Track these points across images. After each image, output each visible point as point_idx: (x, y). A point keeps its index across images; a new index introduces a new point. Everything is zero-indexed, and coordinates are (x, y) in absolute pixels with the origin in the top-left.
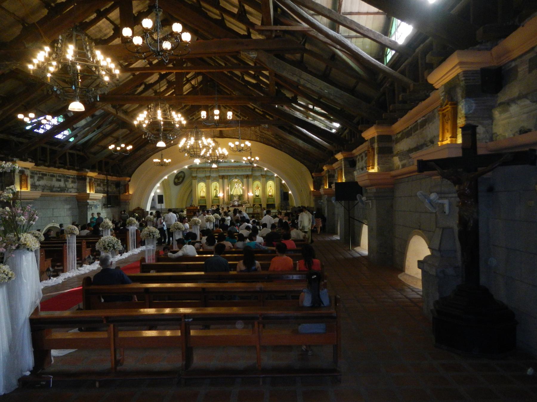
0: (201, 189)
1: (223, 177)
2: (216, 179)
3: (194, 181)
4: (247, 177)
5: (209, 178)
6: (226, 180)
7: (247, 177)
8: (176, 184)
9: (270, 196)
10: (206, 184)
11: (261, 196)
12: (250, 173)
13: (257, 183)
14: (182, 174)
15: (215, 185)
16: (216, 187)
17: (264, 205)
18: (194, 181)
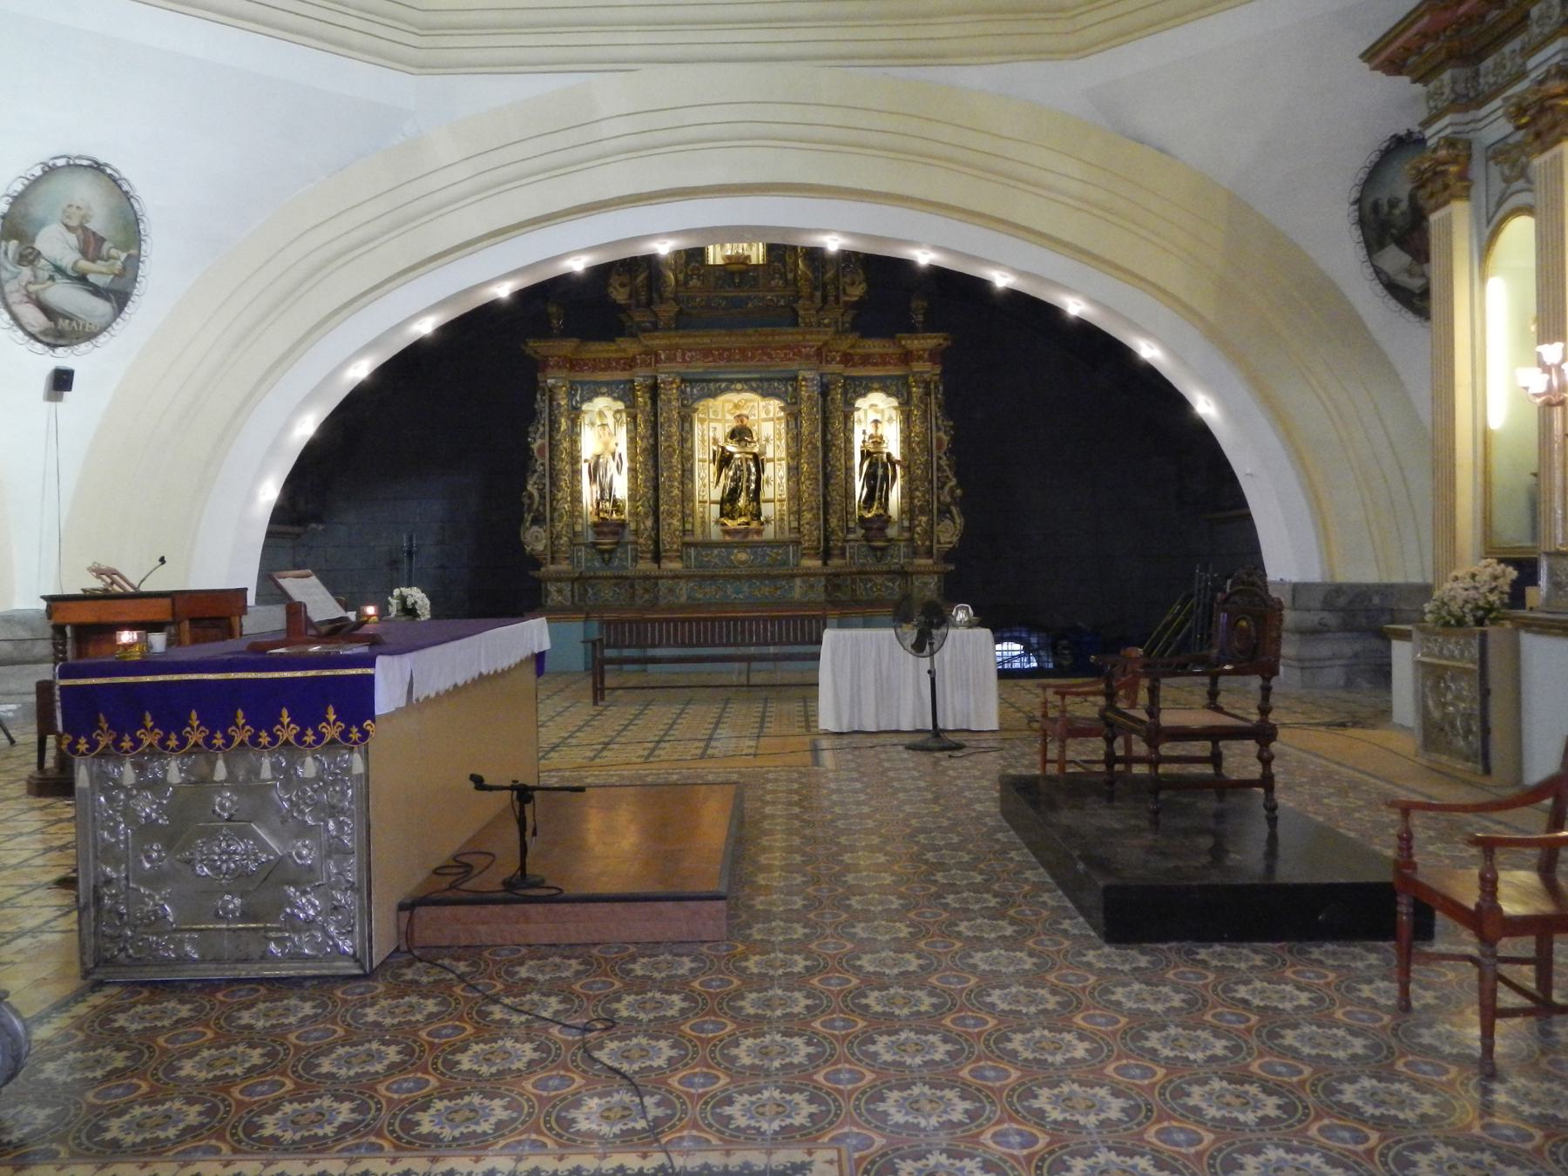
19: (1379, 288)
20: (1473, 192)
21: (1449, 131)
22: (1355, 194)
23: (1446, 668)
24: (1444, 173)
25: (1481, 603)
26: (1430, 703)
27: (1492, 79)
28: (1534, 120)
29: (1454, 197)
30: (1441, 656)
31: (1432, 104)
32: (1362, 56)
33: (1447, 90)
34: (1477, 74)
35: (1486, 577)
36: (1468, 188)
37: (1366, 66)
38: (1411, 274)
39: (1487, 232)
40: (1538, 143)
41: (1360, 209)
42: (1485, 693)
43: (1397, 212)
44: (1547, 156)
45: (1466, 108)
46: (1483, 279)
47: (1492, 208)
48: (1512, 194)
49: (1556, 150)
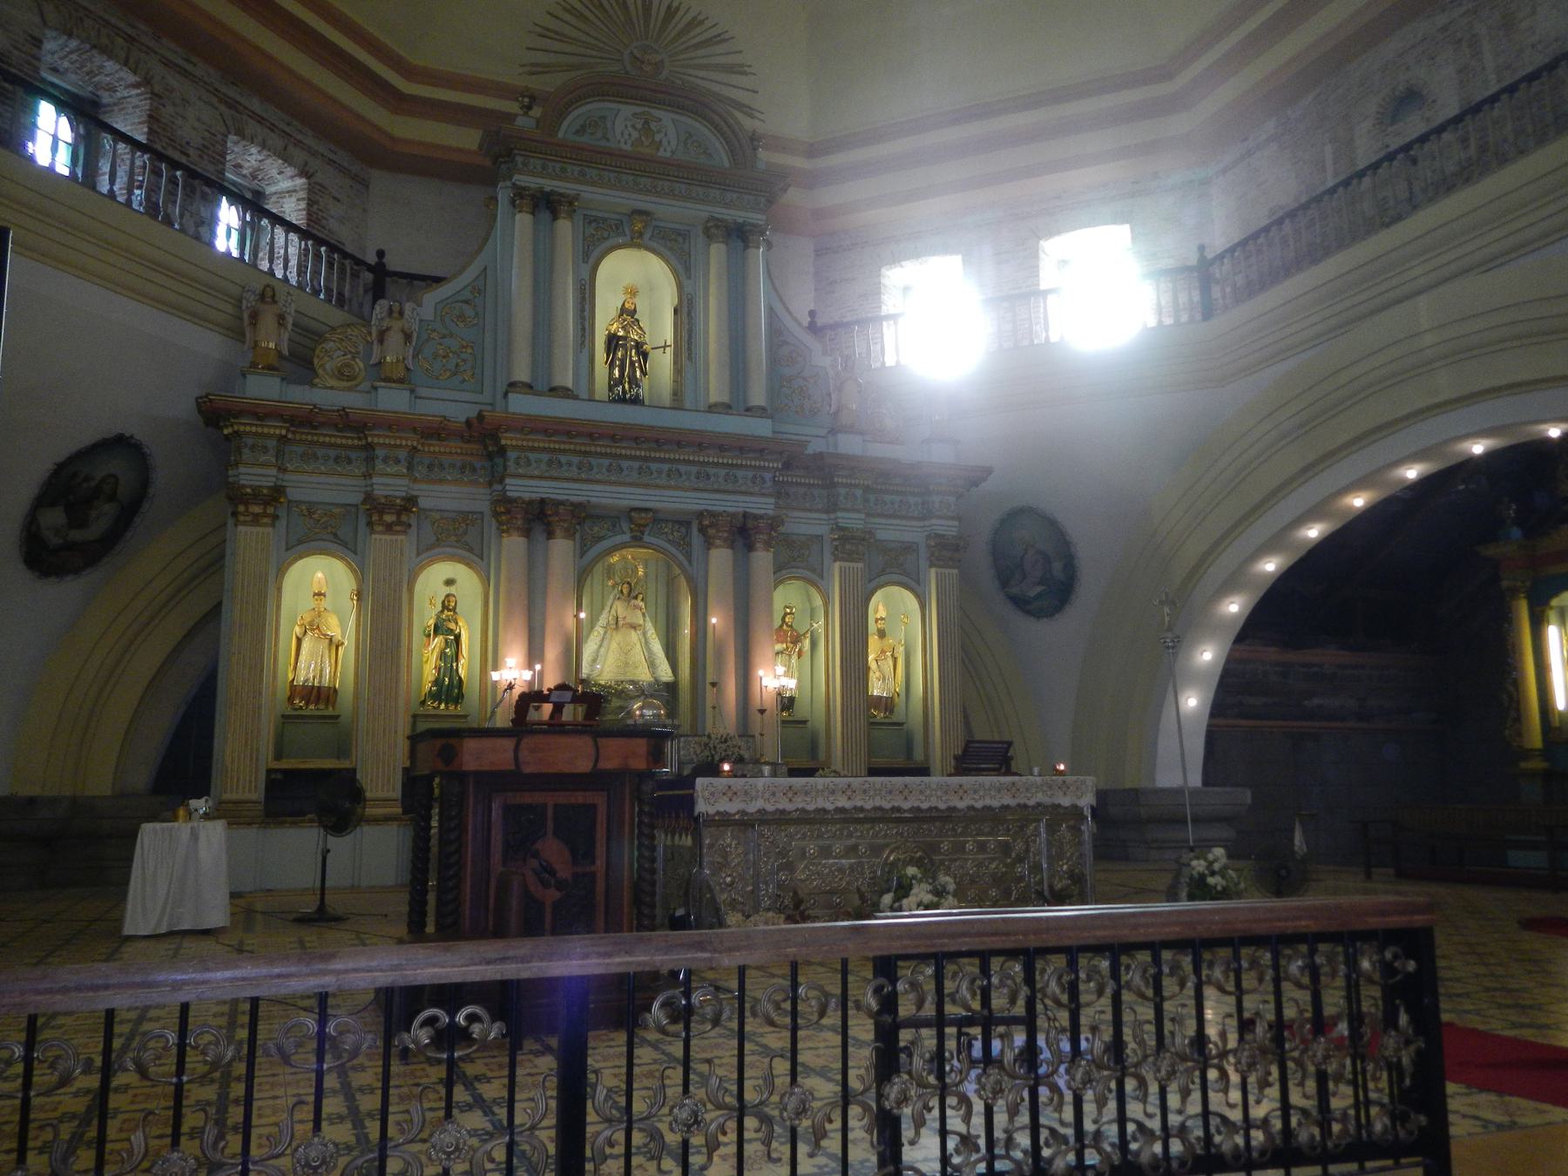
0: (314, 618)
1: (538, 519)
2: (461, 538)
3: (249, 540)
4: (743, 533)
5: (394, 514)
6: (561, 550)
7: (743, 533)
8: (43, 556)
10: (360, 573)
11: (813, 709)
12: (762, 505)
13: (788, 597)
14: (116, 466)
15: (442, 581)
16: (448, 605)
18: (249, 540)
20: (277, 523)
44: (388, 537)
49: (400, 538)
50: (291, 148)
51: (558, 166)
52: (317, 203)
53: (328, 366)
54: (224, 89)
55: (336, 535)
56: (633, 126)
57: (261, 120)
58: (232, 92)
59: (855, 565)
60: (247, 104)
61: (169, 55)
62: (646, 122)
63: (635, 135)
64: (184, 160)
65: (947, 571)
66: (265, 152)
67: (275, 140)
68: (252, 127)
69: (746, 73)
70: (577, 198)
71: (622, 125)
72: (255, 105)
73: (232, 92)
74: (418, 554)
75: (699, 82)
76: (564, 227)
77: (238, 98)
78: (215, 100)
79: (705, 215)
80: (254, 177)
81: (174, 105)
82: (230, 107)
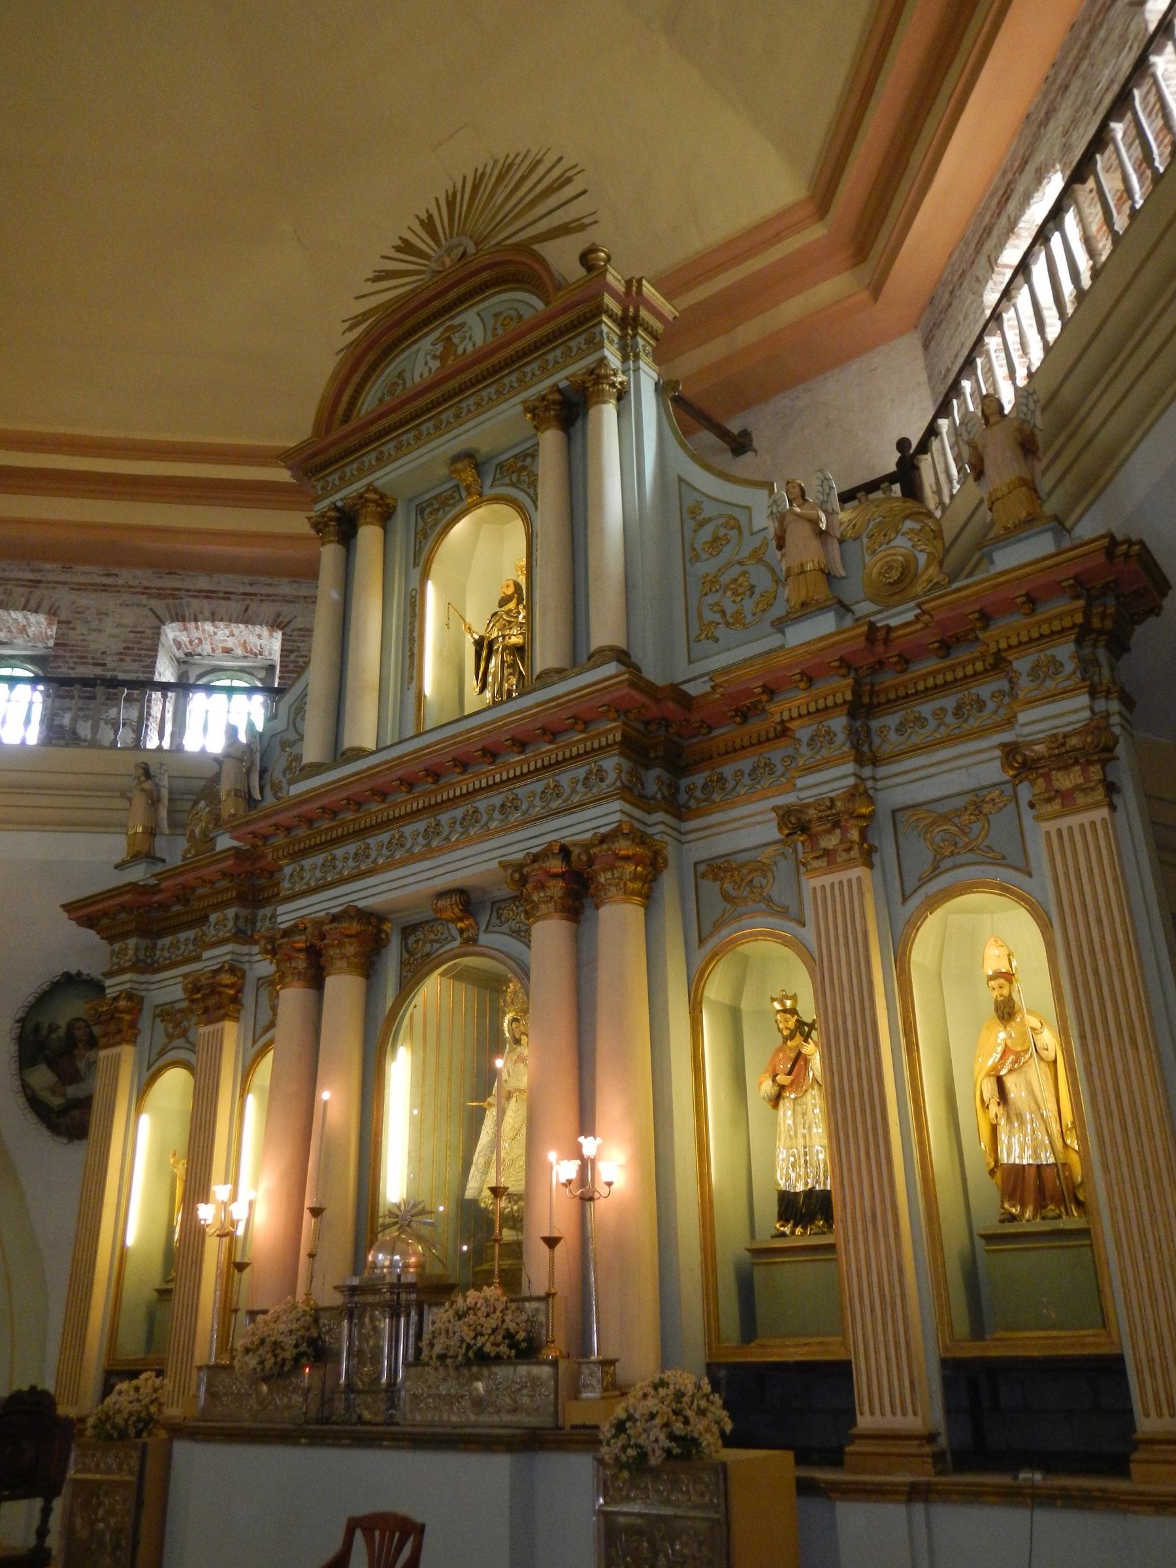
9: (1016, 1182)
17: (897, 1398)
19: (21, 1100)
20: (139, 1039)
21: (128, 985)
22: (21, 1014)
23: (100, 1483)
24: (120, 1020)
25: (143, 1415)
26: (78, 1521)
27: (166, 954)
28: (204, 997)
29: (125, 1041)
30: (97, 1470)
31: (115, 960)
32: (64, 906)
33: (131, 953)
34: (154, 947)
35: (149, 1390)
36: (136, 1036)
37: (66, 915)
38: (53, 1090)
39: (147, 1075)
40: (205, 1016)
41: (22, 1027)
42: (140, 1503)
43: (54, 1036)
44: (211, 1028)
45: (143, 971)
46: (139, 1111)
47: (153, 1057)
48: (173, 1048)
49: (219, 1025)
50: (253, 607)
51: (355, 465)
52: (291, 651)
53: (197, 831)
54: (159, 583)
55: (188, 1042)
56: (434, 357)
57: (209, 595)
58: (171, 582)
59: (844, 876)
60: (191, 586)
61: (82, 579)
62: (449, 339)
63: (435, 364)
64: (98, 671)
65: (1074, 820)
66: (221, 624)
67: (235, 606)
68: (196, 604)
69: (569, 181)
70: (370, 488)
71: (420, 362)
72: (203, 583)
73: (171, 582)
74: (254, 1042)
75: (509, 242)
76: (369, 537)
77: (178, 585)
78: (143, 599)
79: (520, 408)
80: (256, 655)
81: (87, 622)
82: (165, 597)
